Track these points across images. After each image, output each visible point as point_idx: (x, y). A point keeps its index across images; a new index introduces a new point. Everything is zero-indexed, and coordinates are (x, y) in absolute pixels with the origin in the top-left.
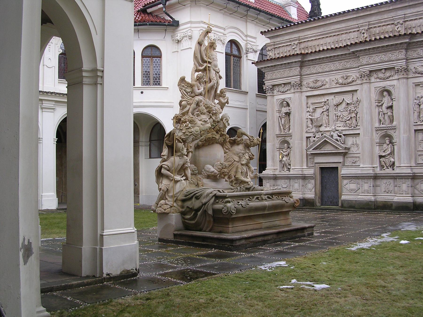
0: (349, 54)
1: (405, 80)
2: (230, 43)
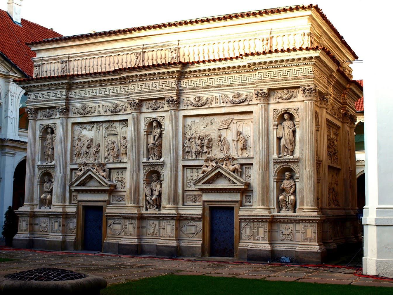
0: (120, 79)
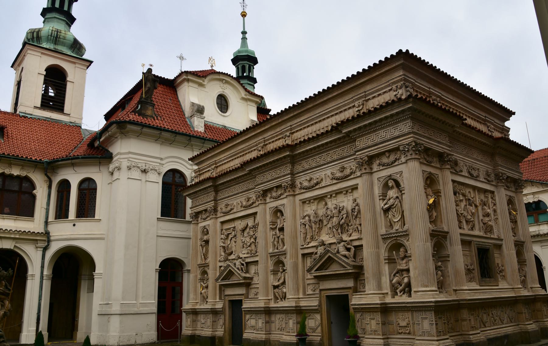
1: (291, 198)
2: (171, 173)
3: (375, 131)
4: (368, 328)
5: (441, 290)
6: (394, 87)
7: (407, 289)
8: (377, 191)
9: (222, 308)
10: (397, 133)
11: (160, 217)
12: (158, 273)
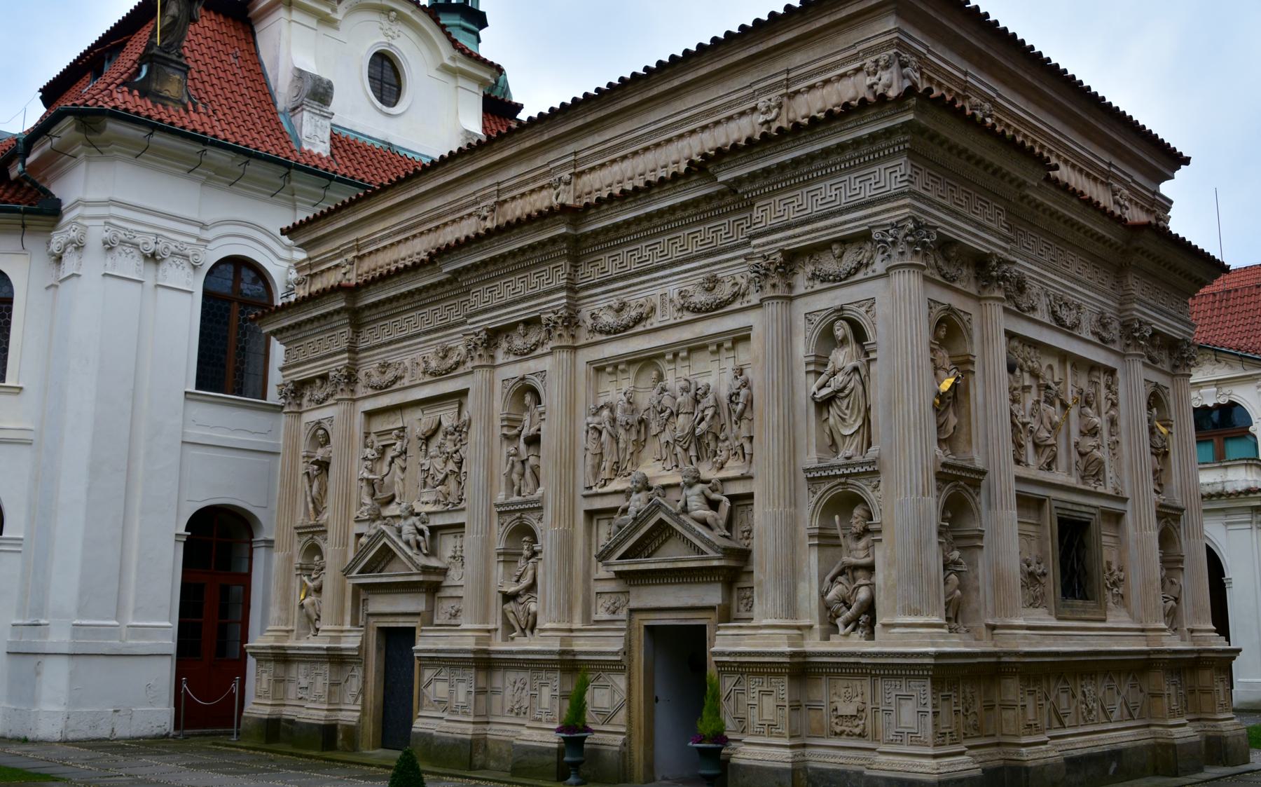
1: (565, 355)
2: (231, 268)
3: (807, 183)
4: (753, 717)
5: (954, 625)
6: (869, 62)
7: (863, 618)
8: (802, 348)
9: (360, 648)
10: (867, 193)
11: (192, 389)
12: (182, 545)
